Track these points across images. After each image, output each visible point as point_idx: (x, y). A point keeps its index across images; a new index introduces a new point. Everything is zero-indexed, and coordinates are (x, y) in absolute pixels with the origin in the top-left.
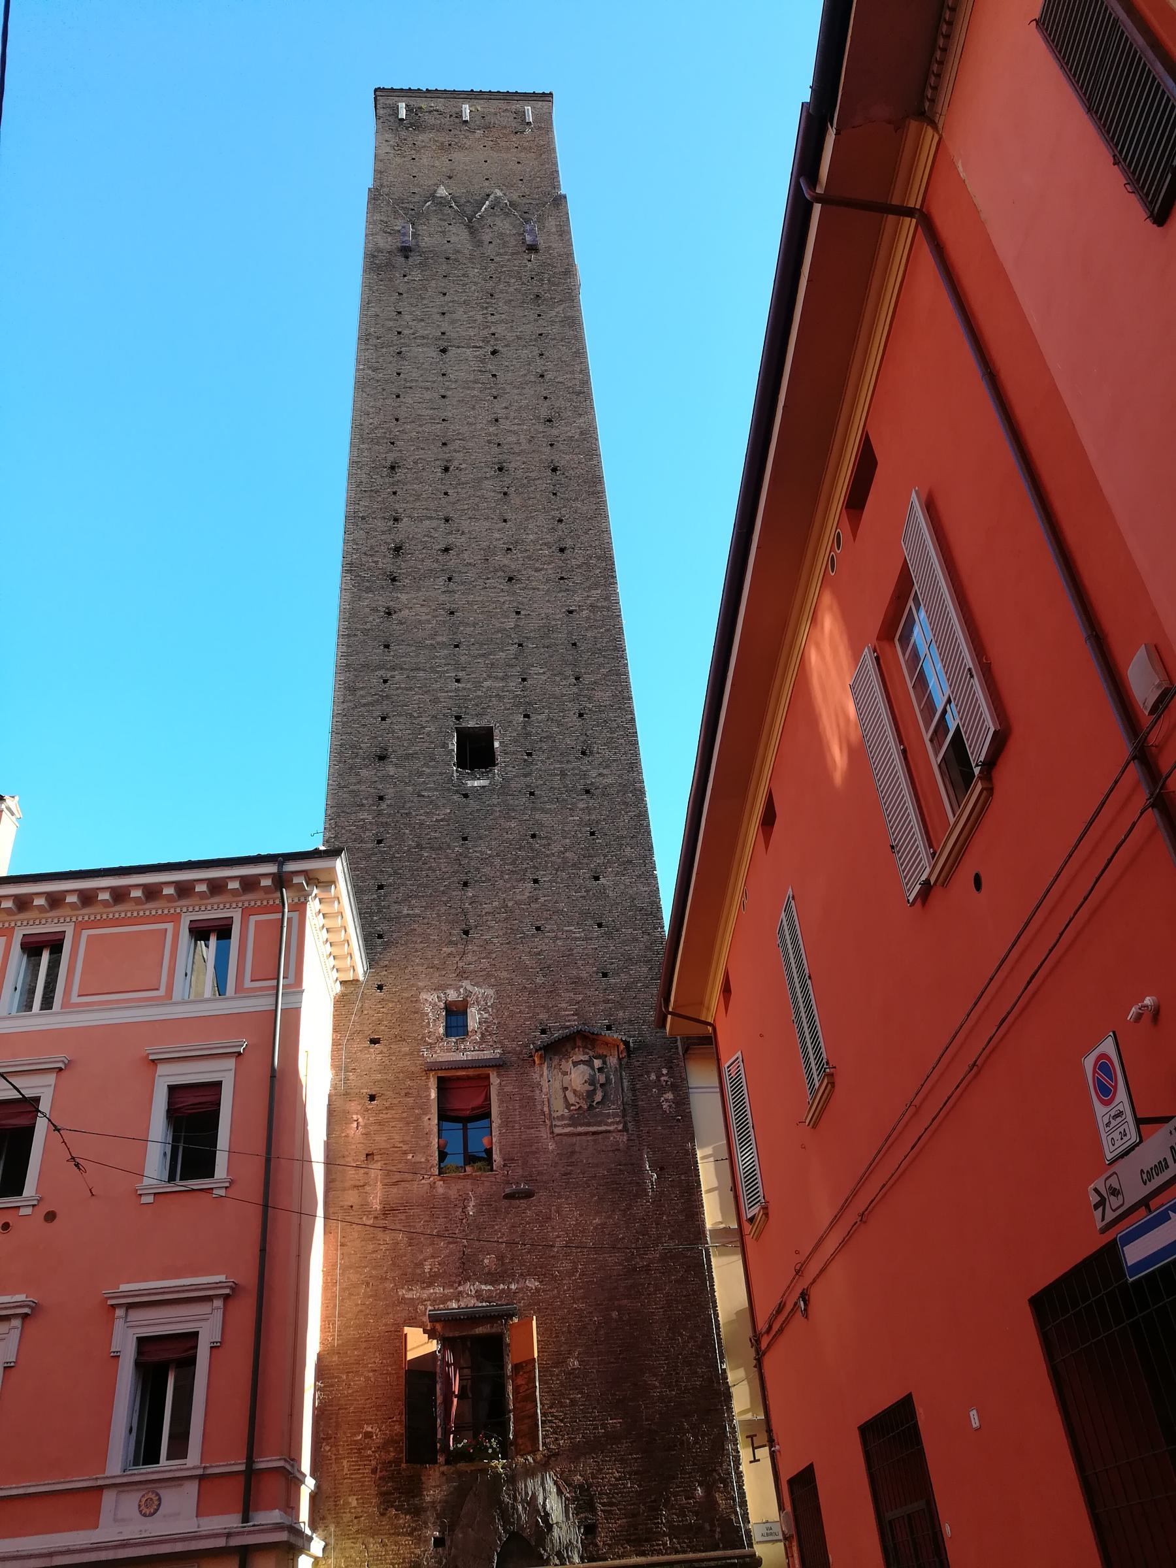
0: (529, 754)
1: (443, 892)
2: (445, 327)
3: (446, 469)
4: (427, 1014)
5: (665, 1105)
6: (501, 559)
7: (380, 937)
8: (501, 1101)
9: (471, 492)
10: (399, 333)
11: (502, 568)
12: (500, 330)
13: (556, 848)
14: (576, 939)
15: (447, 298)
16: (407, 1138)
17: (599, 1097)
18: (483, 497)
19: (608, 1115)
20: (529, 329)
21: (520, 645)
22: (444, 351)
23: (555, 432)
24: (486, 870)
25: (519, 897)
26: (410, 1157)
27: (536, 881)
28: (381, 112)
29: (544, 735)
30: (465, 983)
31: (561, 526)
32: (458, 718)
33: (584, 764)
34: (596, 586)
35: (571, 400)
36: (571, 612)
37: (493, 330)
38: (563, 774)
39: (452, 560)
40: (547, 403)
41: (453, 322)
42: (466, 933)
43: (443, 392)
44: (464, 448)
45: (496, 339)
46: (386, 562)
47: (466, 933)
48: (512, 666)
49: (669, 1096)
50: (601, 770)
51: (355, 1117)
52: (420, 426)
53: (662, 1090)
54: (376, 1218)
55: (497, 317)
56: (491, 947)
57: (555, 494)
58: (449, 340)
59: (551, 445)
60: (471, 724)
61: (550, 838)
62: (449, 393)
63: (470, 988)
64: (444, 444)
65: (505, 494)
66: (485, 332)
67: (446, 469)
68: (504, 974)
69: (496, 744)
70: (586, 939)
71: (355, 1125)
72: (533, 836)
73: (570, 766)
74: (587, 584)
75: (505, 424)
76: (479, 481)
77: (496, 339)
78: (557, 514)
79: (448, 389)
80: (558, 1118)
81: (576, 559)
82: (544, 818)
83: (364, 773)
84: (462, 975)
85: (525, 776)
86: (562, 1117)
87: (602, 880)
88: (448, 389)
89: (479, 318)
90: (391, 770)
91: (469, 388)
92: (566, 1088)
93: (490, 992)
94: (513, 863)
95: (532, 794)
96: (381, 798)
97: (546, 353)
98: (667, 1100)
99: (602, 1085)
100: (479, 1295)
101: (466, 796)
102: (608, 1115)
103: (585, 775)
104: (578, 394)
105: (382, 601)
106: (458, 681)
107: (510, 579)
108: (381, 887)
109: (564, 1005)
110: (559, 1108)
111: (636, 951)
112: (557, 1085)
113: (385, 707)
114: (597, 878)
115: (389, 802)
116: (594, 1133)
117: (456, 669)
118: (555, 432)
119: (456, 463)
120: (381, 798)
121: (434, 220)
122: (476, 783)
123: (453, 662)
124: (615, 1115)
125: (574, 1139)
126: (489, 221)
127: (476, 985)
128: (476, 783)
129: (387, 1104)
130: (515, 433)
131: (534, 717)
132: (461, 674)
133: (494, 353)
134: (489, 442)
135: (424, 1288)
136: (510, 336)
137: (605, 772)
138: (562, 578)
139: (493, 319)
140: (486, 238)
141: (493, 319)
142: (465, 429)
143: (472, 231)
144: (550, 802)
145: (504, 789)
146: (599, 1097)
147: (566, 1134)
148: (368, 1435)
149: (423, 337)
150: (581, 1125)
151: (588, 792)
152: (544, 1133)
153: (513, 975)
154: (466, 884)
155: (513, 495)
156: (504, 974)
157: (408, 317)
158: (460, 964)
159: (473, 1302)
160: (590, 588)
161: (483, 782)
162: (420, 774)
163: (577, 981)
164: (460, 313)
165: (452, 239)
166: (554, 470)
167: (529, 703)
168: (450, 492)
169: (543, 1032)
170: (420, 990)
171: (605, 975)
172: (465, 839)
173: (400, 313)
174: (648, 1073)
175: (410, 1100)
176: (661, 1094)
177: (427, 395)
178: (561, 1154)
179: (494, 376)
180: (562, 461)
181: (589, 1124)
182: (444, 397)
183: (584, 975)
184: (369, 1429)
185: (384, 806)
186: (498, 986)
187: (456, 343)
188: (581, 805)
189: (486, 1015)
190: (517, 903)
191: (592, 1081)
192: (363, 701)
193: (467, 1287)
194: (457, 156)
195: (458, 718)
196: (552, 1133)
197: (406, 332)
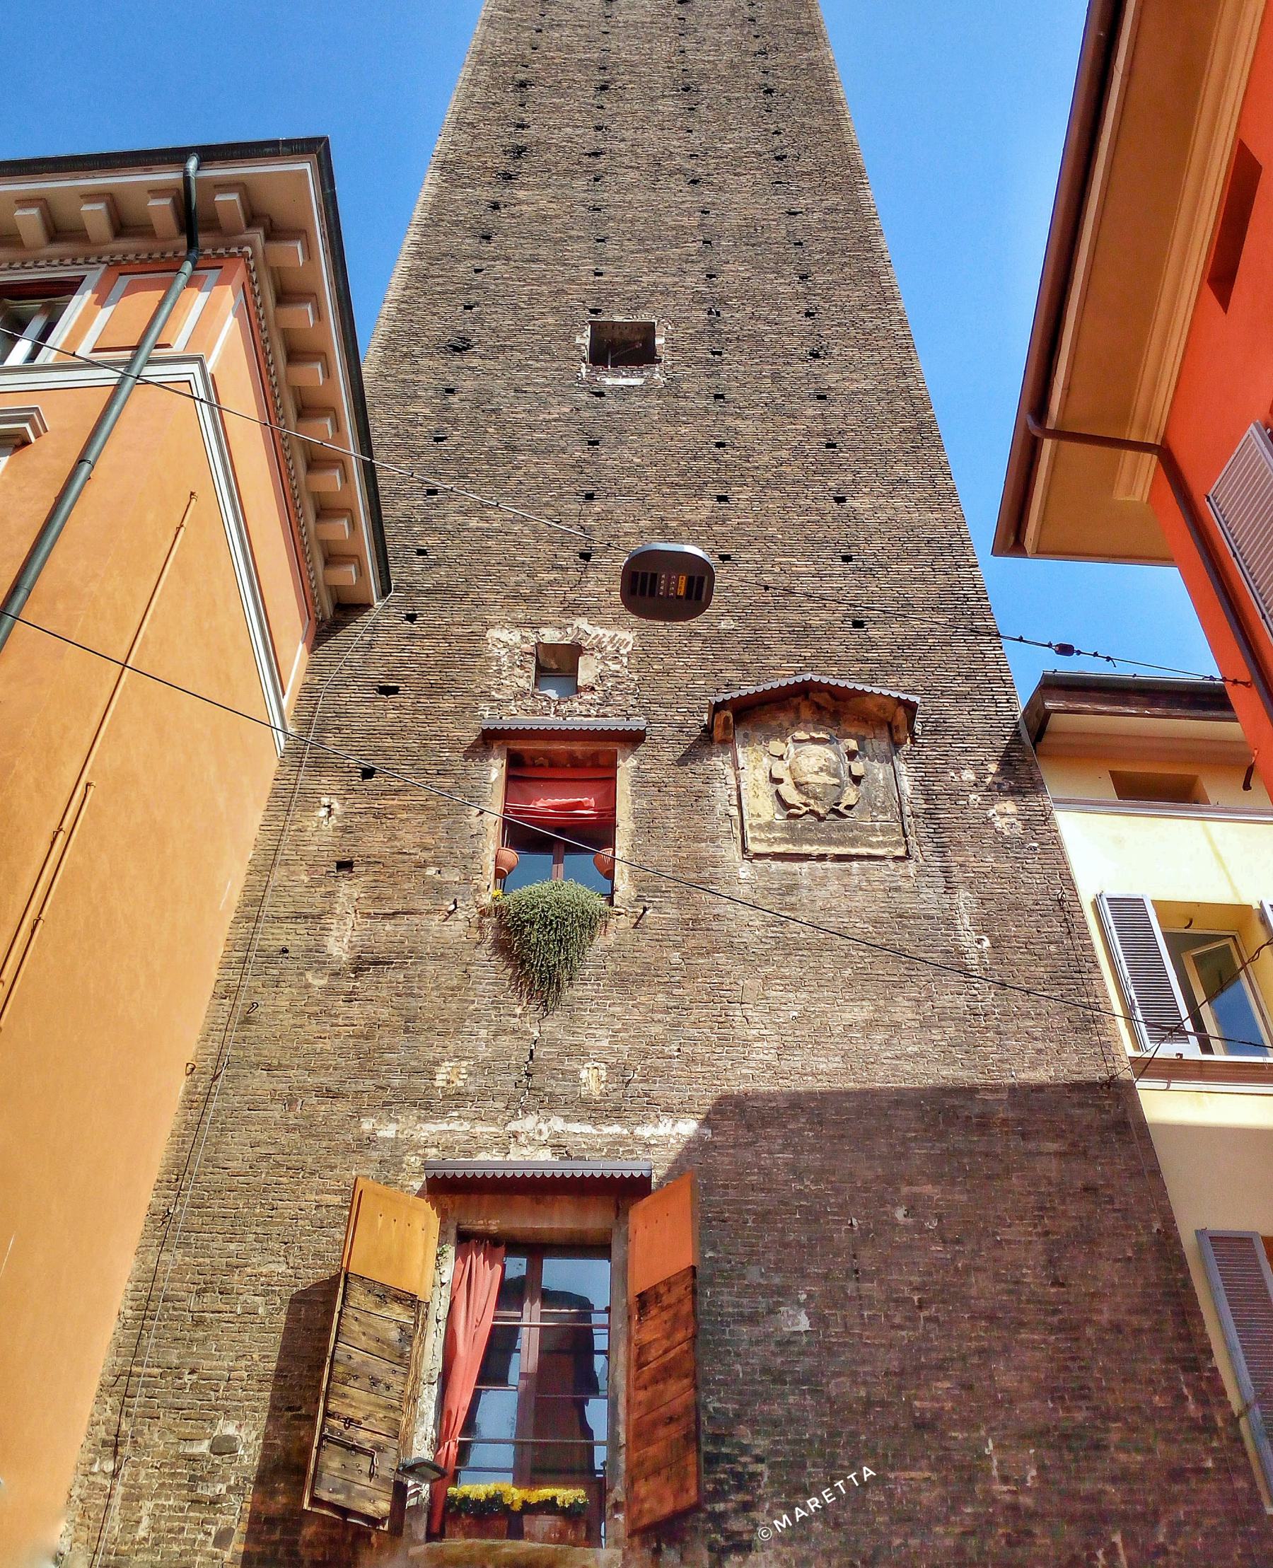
1: (547, 504)
4: (498, 659)
5: (1000, 823)
7: (421, 552)
8: (637, 794)
14: (798, 575)
16: (429, 840)
19: (873, 831)
25: (688, 517)
26: (431, 871)
27: (722, 499)
30: (582, 623)
33: (816, 366)
38: (776, 377)
39: (602, 163)
42: (586, 556)
46: (502, 163)
47: (586, 556)
51: (325, 800)
54: (336, 974)
60: (618, 318)
69: (659, 341)
70: (817, 575)
71: (323, 812)
72: (719, 445)
73: (790, 369)
80: (760, 827)
83: (424, 362)
84: (572, 609)
86: (770, 826)
87: (850, 502)
90: (476, 362)
92: (780, 781)
94: (682, 474)
96: (450, 391)
98: (1003, 815)
101: (601, 395)
105: (485, 195)
108: (433, 492)
109: (773, 661)
110: (761, 807)
111: (917, 592)
112: (762, 776)
113: (473, 298)
114: (840, 500)
115: (463, 396)
116: (839, 858)
117: (596, 263)
120: (450, 391)
122: (622, 382)
125: (795, 866)
127: (602, 624)
128: (622, 382)
129: (396, 784)
131: (724, 314)
135: (425, 1120)
145: (672, 389)
148: (223, 1447)
150: (810, 842)
152: (732, 851)
154: (590, 497)
158: (571, 596)
159: (545, 1155)
162: (521, 367)
163: (803, 633)
170: (488, 626)
171: (858, 624)
174: (958, 770)
175: (448, 782)
178: (769, 889)
181: (830, 842)
183: (815, 622)
184: (230, 1430)
185: (453, 399)
188: (810, 412)
189: (615, 667)
190: (685, 524)
192: (439, 289)
193: (527, 1124)
196: (745, 850)
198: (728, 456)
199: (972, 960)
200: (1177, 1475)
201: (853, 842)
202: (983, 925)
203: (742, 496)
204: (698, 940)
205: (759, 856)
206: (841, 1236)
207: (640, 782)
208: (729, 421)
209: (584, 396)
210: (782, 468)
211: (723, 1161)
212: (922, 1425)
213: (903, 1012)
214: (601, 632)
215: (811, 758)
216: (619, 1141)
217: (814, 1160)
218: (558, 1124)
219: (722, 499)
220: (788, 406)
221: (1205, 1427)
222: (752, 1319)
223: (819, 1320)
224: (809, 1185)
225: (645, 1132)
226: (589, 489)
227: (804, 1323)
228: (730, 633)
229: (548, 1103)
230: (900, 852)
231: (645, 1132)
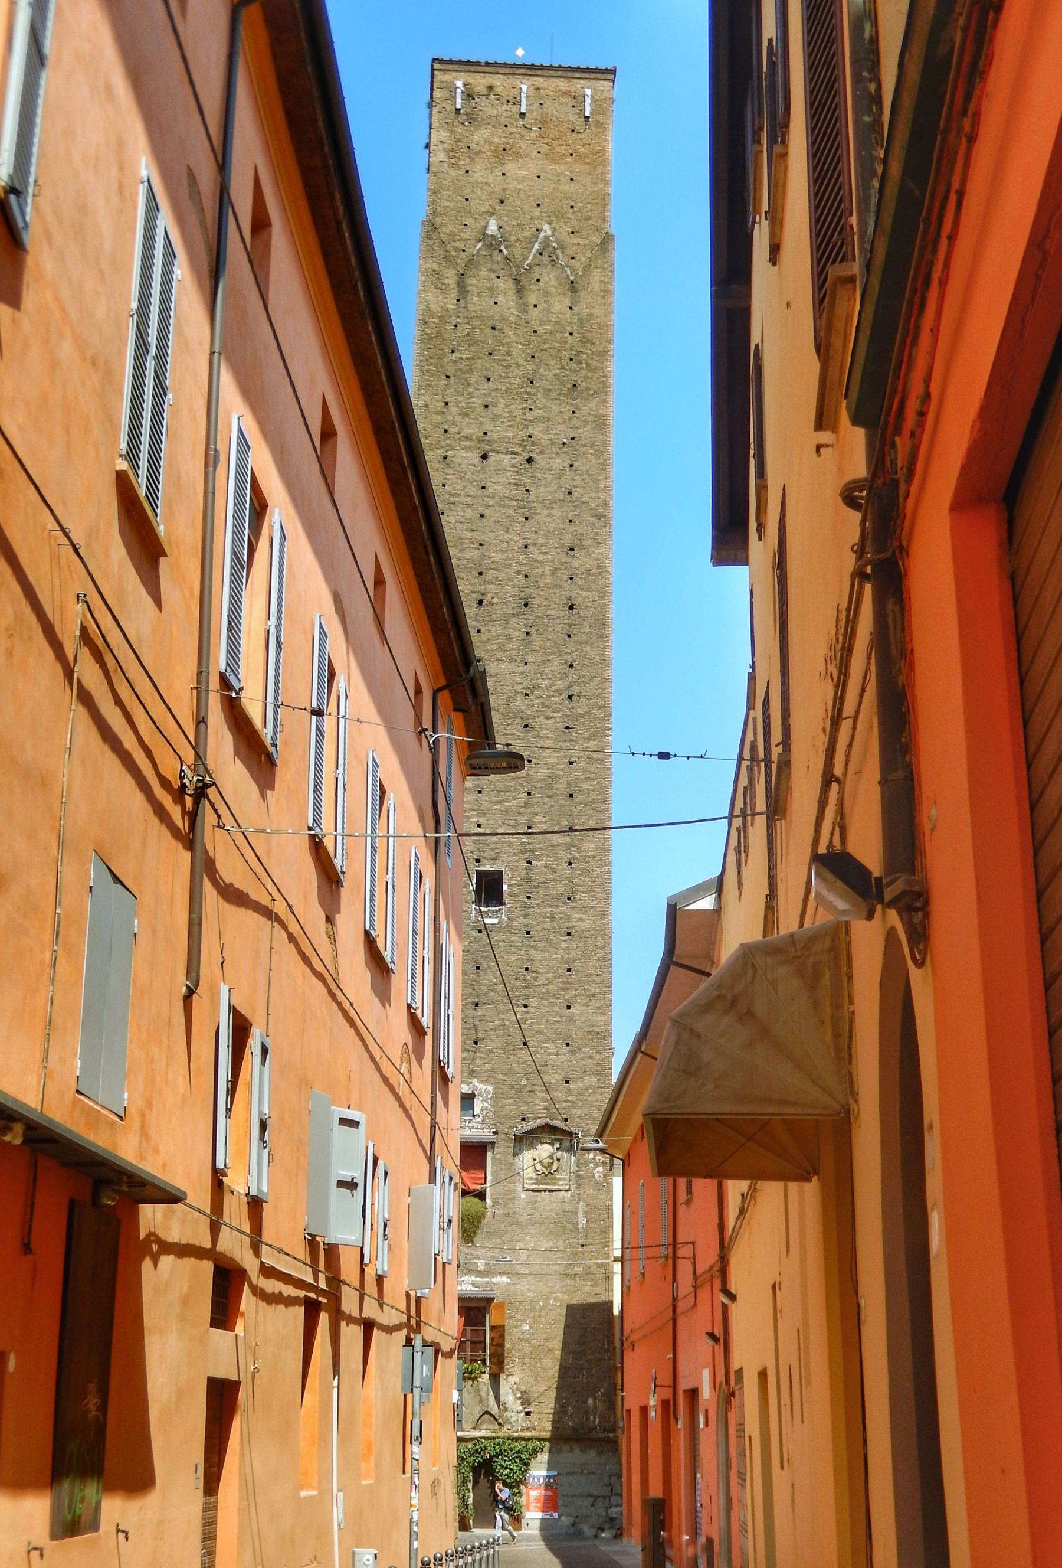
0: (529, 898)
2: (488, 426)
3: (481, 602)
6: (520, 704)
9: (500, 630)
10: (446, 431)
11: (518, 715)
12: (536, 430)
13: (542, 980)
14: (550, 1054)
15: (491, 385)
17: (554, 1168)
18: (510, 638)
19: (560, 1179)
20: (562, 432)
21: (529, 794)
22: (484, 457)
23: (575, 563)
24: (491, 994)
27: (526, 1006)
28: (437, 94)
29: (542, 880)
30: (475, 1081)
31: (572, 671)
32: (478, 861)
34: (593, 737)
35: (593, 525)
36: (571, 763)
37: (530, 430)
38: (552, 917)
40: (572, 528)
41: (496, 417)
42: (476, 1043)
43: (481, 510)
44: (497, 579)
45: (533, 444)
47: (476, 1043)
48: (520, 814)
49: (601, 1169)
50: (580, 916)
52: (461, 550)
53: (596, 1165)
55: (535, 413)
56: (492, 1055)
57: (569, 636)
58: (490, 443)
59: (571, 579)
60: (488, 868)
61: (538, 972)
62: (487, 512)
63: (477, 1084)
64: (480, 574)
65: (528, 634)
66: (523, 434)
67: (481, 602)
68: (500, 1076)
69: (505, 887)
70: (557, 1055)
72: (527, 969)
74: (587, 735)
75: (534, 553)
76: (507, 618)
77: (533, 444)
78: (569, 658)
79: (487, 506)
81: (581, 706)
82: (537, 955)
85: (526, 916)
86: (530, 1179)
88: (487, 506)
89: (518, 413)
91: (504, 506)
93: (490, 1088)
95: (528, 933)
97: (576, 464)
99: (558, 1160)
100: (473, 1285)
102: (560, 1179)
103: (569, 919)
104: (599, 517)
106: (479, 826)
107: (526, 726)
109: (537, 1102)
110: (530, 1173)
114: (569, 1007)
116: (550, 1191)
118: (575, 563)
119: (489, 596)
121: (484, 273)
123: (476, 807)
124: (565, 1179)
126: (537, 272)
130: (542, 563)
132: (482, 820)
133: (530, 460)
134: (518, 572)
136: (544, 439)
137: (584, 917)
138: (567, 728)
139: (529, 415)
140: (532, 299)
141: (529, 415)
142: (499, 557)
144: (542, 940)
145: (509, 929)
146: (554, 1168)
147: (533, 1190)
149: (467, 438)
151: (569, 934)
152: (519, 1187)
153: (505, 1078)
154: (477, 1005)
155: (534, 635)
156: (500, 1076)
157: (454, 410)
159: (470, 1287)
160: (589, 739)
161: (495, 921)
164: (500, 408)
165: (500, 299)
166: (571, 608)
167: (533, 851)
168: (483, 629)
169: (523, 1119)
172: (478, 968)
173: (447, 404)
176: (594, 1168)
177: (469, 513)
179: (528, 491)
180: (580, 596)
181: (546, 1184)
182: (482, 516)
186: (496, 1085)
187: (495, 446)
188: (564, 945)
191: (551, 1157)
193: (465, 1278)
194: (512, 168)
195: (478, 861)
197: (452, 430)
198: (530, 976)
199: (580, 1227)
200: (599, 1360)
201: (554, 1184)
202: (586, 1214)
203: (533, 1002)
204: (509, 1220)
205: (528, 1190)
206: (538, 1307)
207: (494, 1159)
208: (532, 952)
209: (474, 933)
210: (550, 986)
211: (512, 1288)
212: (550, 1350)
213: (561, 1243)
214: (481, 1086)
215: (545, 1150)
216: (487, 1283)
217: (533, 1287)
218: (473, 1278)
219: (526, 1006)
220: (556, 941)
221: (608, 1350)
222: (516, 1327)
223: (531, 1327)
224: (531, 1294)
225: (494, 1280)
226: (476, 1000)
227: (527, 1328)
228: (525, 1086)
229: (470, 1272)
230: (567, 1188)
231: (494, 1280)
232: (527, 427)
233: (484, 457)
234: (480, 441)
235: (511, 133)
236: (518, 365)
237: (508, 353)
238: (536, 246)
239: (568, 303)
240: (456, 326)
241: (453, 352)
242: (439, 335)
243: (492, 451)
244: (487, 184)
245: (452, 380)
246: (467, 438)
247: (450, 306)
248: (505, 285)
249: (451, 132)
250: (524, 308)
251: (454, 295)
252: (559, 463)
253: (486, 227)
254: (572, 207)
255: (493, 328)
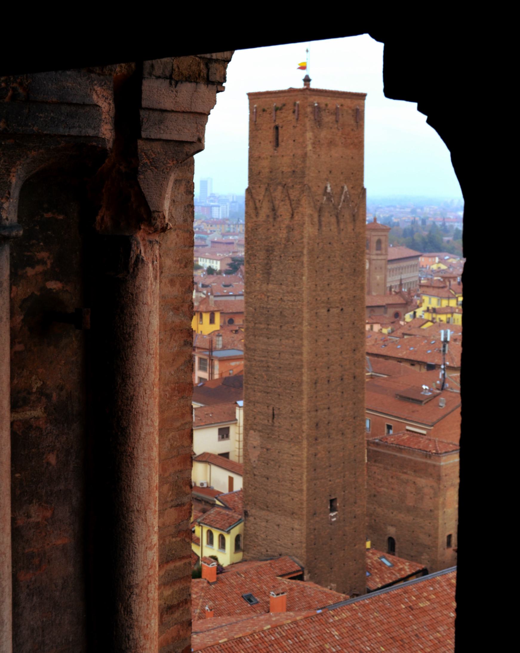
22: (328, 310)
52: (323, 358)
55: (344, 286)
66: (340, 297)
79: (330, 335)
88: (330, 335)
121: (326, 214)
133: (342, 309)
140: (342, 226)
143: (338, 222)
149: (323, 302)
157: (319, 288)
165: (332, 228)
166: (354, 377)
197: (319, 299)
232: (340, 293)
233: (328, 310)
234: (327, 303)
235: (333, 132)
236: (338, 262)
237: (335, 257)
238: (343, 197)
239: (352, 228)
240: (318, 244)
241: (318, 258)
242: (313, 250)
243: (332, 307)
244: (325, 162)
245: (318, 273)
246: (323, 302)
247: (316, 233)
248: (333, 220)
249: (313, 132)
250: (340, 231)
251: (317, 228)
252: (351, 309)
253: (326, 188)
254: (352, 173)
255: (330, 243)
